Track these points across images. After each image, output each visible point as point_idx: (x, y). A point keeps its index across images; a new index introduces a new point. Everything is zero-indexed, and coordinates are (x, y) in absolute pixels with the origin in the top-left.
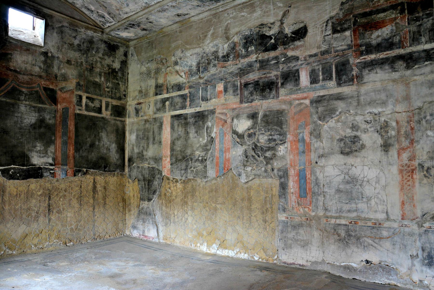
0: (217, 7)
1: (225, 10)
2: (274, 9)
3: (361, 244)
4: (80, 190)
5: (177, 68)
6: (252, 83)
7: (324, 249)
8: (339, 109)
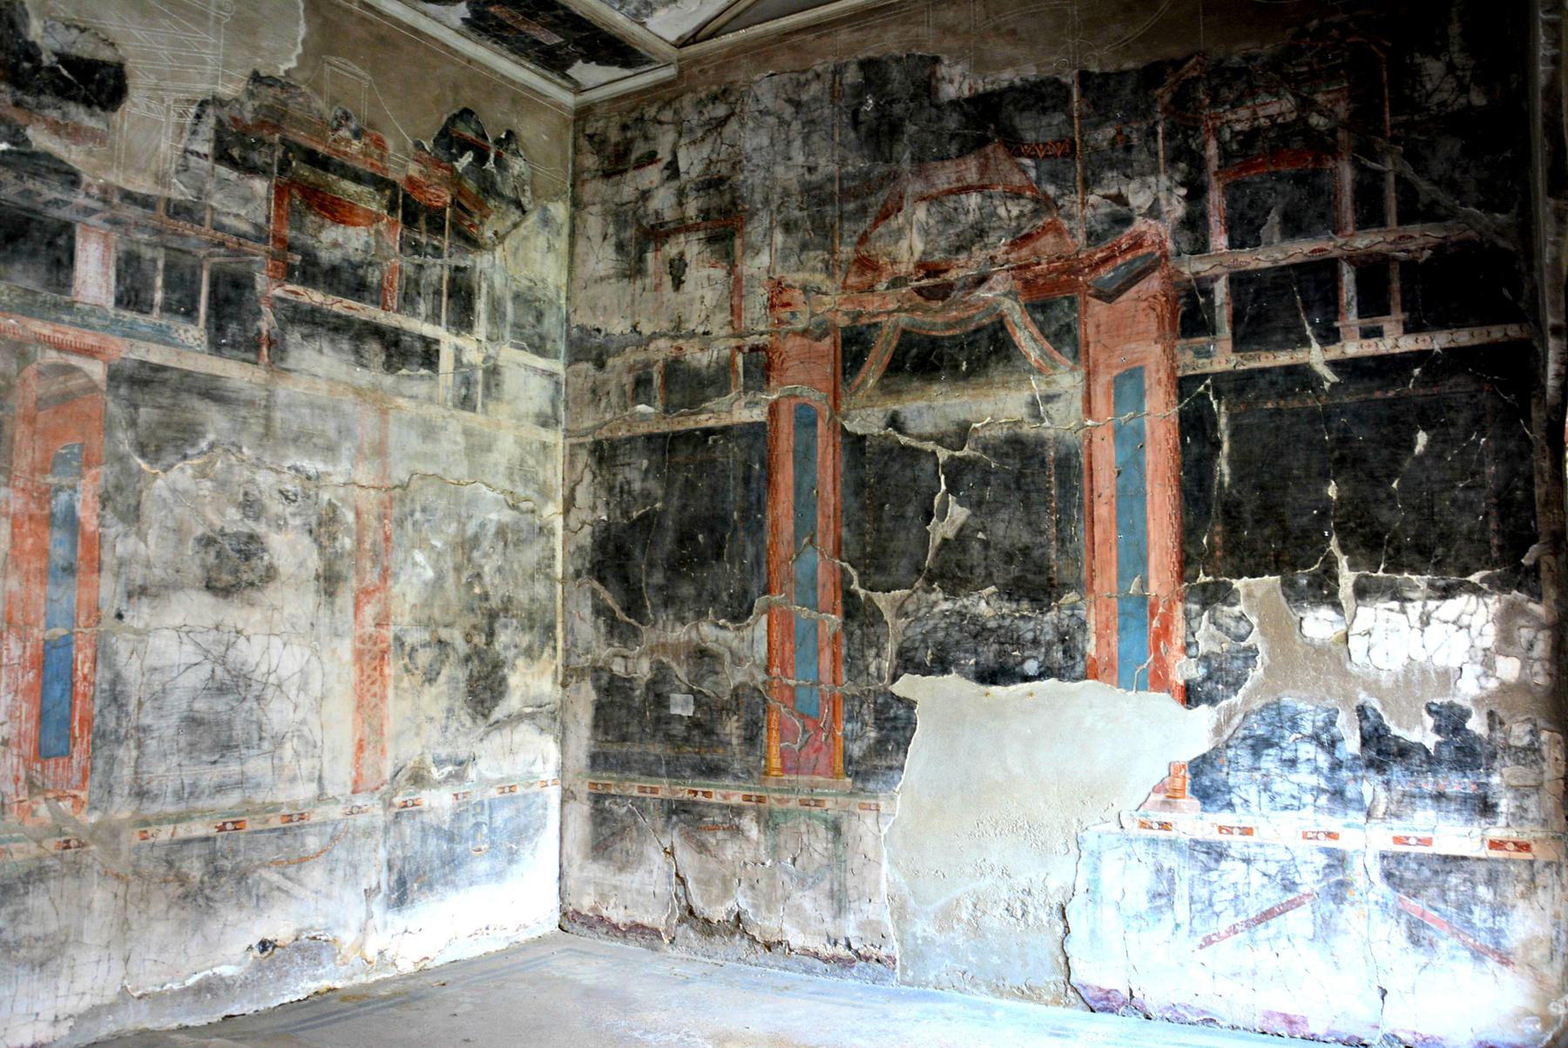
3: (249, 893)
7: (129, 946)
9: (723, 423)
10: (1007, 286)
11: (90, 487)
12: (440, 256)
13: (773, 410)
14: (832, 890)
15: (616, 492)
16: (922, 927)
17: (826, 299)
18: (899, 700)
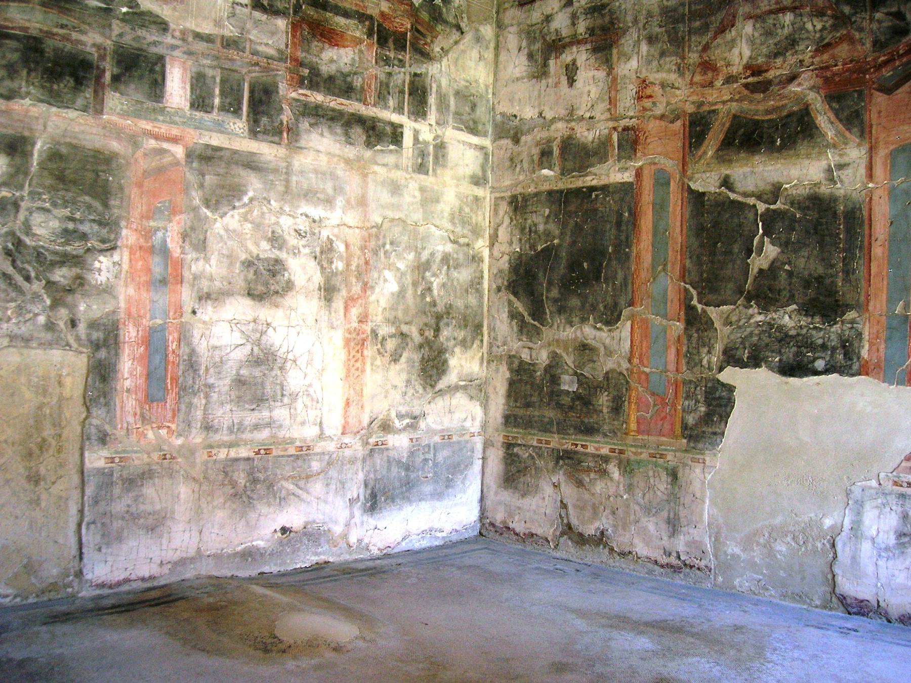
3: (275, 497)
7: (202, 523)
9: (602, 183)
10: (812, 82)
11: (175, 228)
12: (403, 66)
13: (639, 174)
14: (669, 518)
15: (527, 232)
16: (733, 548)
17: (678, 92)
18: (723, 385)
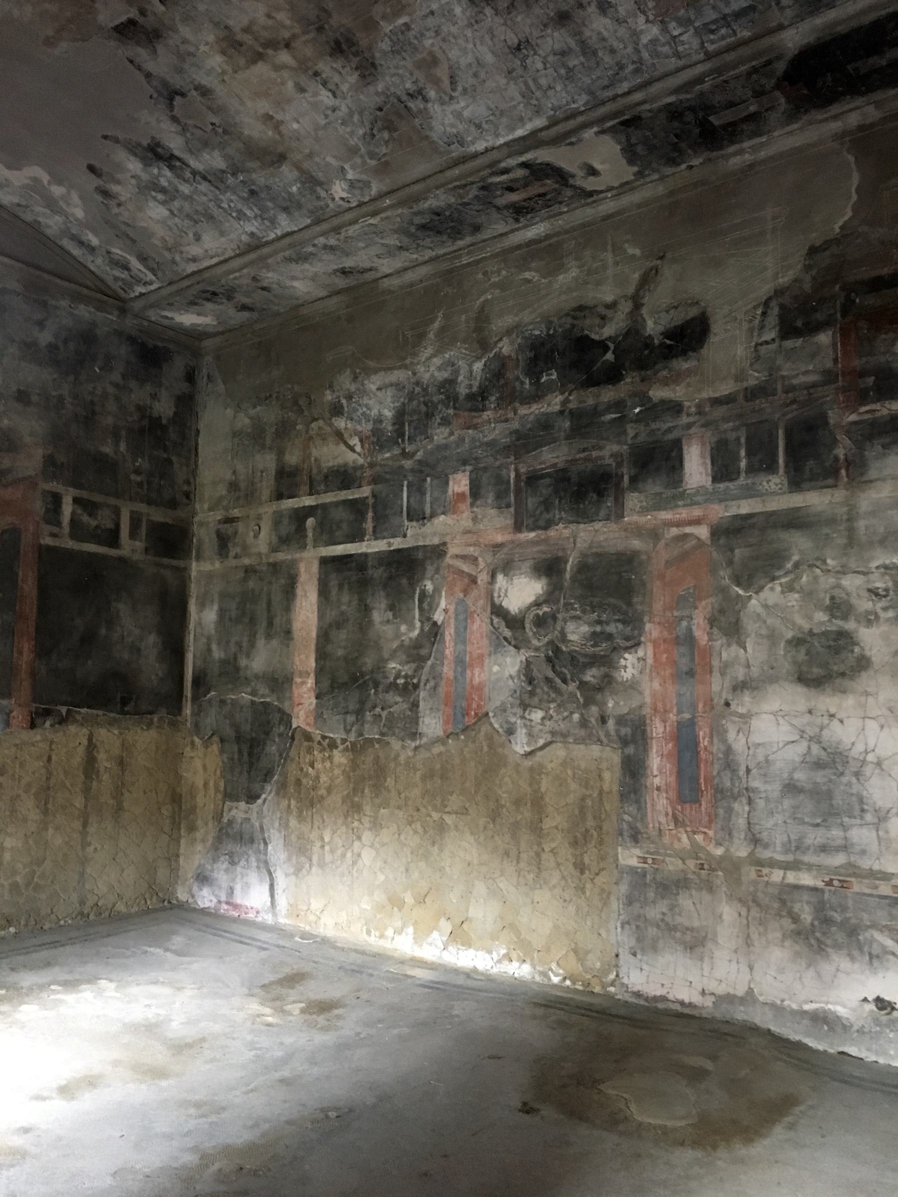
0: (455, 251)
1: (477, 262)
2: (617, 264)
3: (860, 949)
4: (48, 770)
5: (341, 423)
6: (548, 475)
8: (793, 555)
